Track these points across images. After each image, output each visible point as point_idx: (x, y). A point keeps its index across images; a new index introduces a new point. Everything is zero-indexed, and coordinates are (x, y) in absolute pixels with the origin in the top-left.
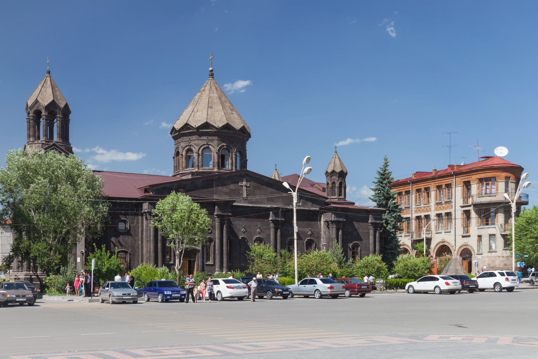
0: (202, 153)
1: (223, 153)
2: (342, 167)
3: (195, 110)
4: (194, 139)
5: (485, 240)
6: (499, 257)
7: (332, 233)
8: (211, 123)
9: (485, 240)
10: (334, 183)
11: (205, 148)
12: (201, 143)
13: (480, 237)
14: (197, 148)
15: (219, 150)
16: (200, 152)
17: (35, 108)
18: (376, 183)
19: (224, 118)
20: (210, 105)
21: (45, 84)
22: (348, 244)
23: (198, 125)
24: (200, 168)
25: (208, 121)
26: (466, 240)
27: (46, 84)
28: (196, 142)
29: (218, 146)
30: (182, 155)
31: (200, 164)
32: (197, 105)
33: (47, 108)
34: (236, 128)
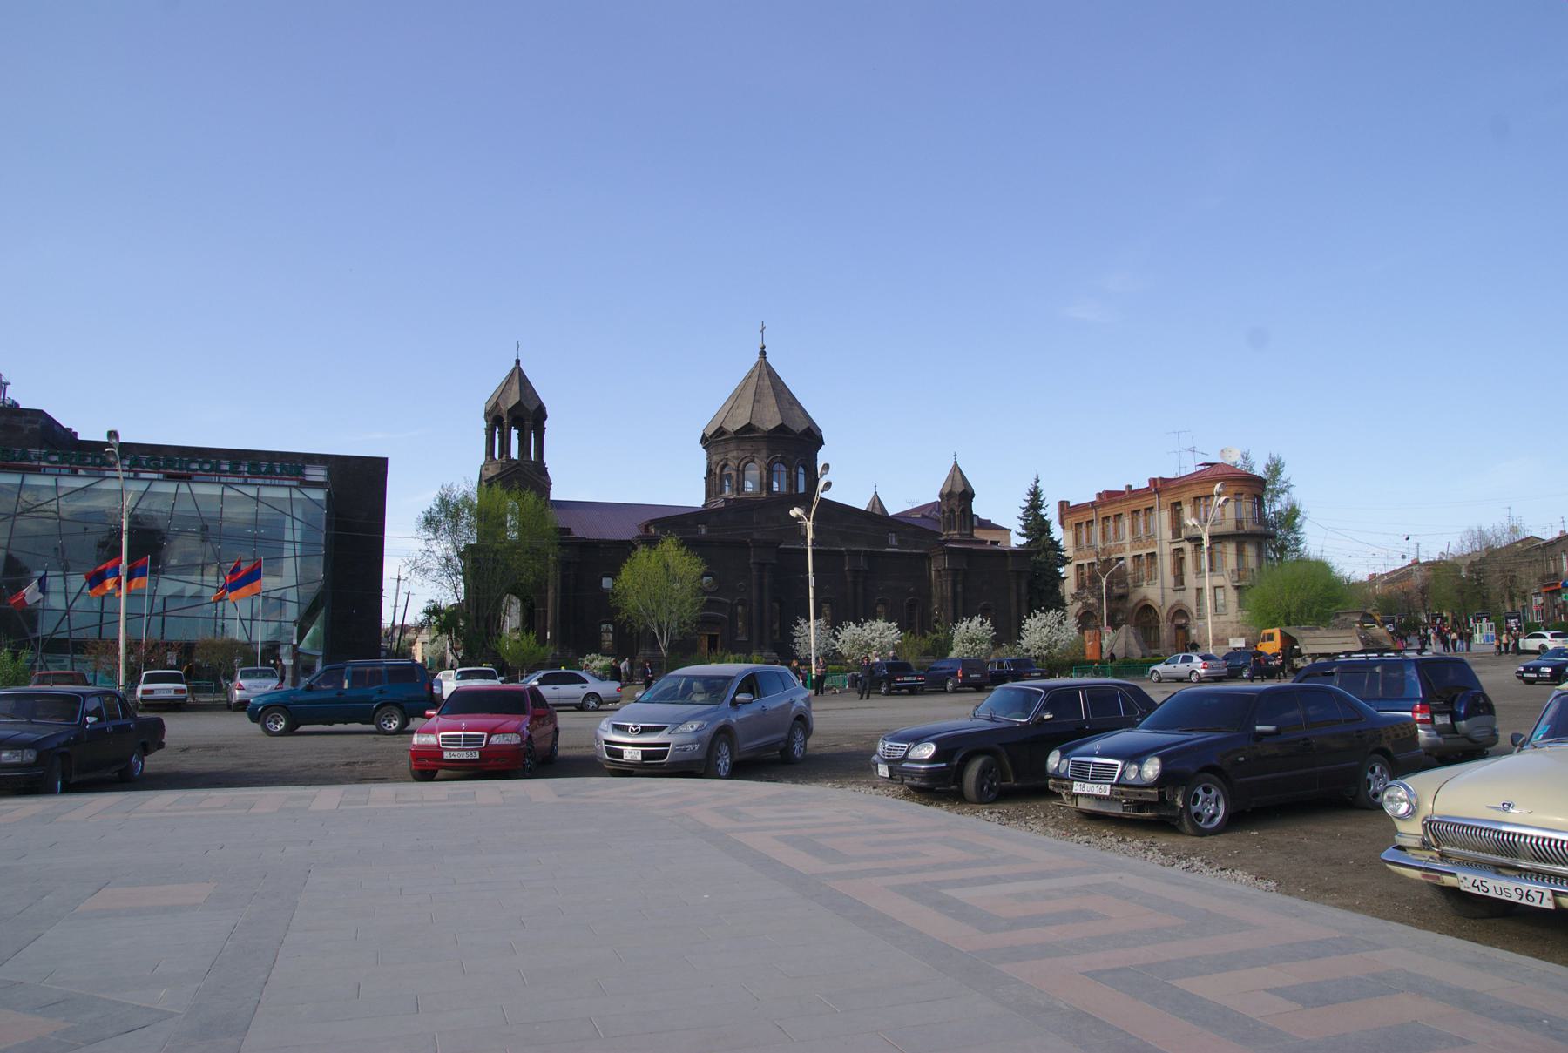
2: (965, 485)
8: (757, 424)
10: (952, 511)
14: (736, 462)
17: (495, 414)
18: (1023, 508)
19: (778, 417)
20: (757, 398)
23: (737, 427)
25: (752, 423)
26: (1178, 596)
27: (513, 379)
28: (735, 453)
30: (715, 473)
31: (740, 487)
33: (510, 411)
34: (796, 430)
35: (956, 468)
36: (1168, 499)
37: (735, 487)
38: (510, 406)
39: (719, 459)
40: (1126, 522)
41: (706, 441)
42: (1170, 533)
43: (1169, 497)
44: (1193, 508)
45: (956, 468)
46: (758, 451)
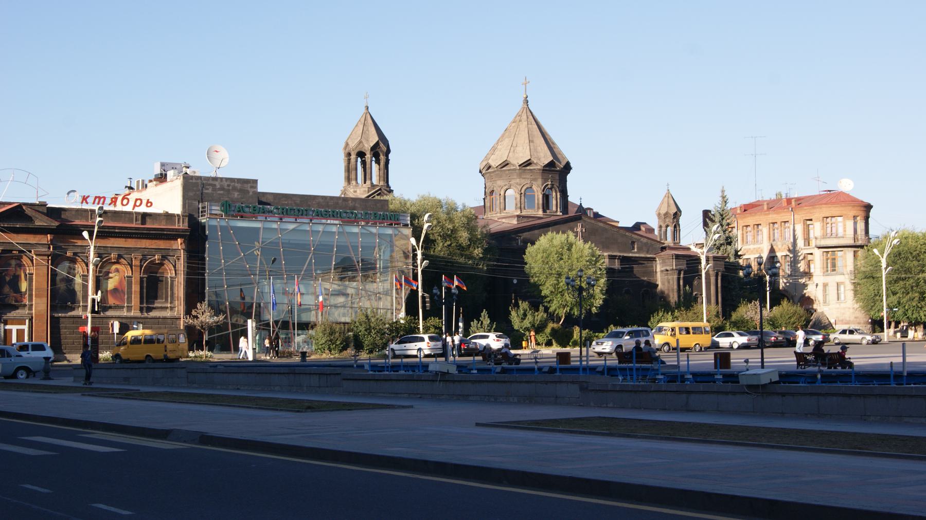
0: (525, 194)
1: (547, 193)
3: (514, 145)
4: (515, 177)
5: (832, 290)
6: (849, 308)
7: (673, 283)
9: (832, 290)
11: (527, 188)
12: (523, 182)
13: (825, 285)
15: (543, 191)
16: (523, 192)
21: (366, 122)
22: (656, 292)
24: (523, 210)
28: (518, 180)
29: (542, 185)
31: (522, 206)
32: (515, 138)
35: (669, 196)
36: (800, 216)
37: (519, 205)
38: (372, 145)
39: (503, 184)
40: (765, 230)
41: (486, 171)
42: (803, 241)
43: (802, 215)
44: (822, 225)
45: (669, 196)
46: (535, 180)
